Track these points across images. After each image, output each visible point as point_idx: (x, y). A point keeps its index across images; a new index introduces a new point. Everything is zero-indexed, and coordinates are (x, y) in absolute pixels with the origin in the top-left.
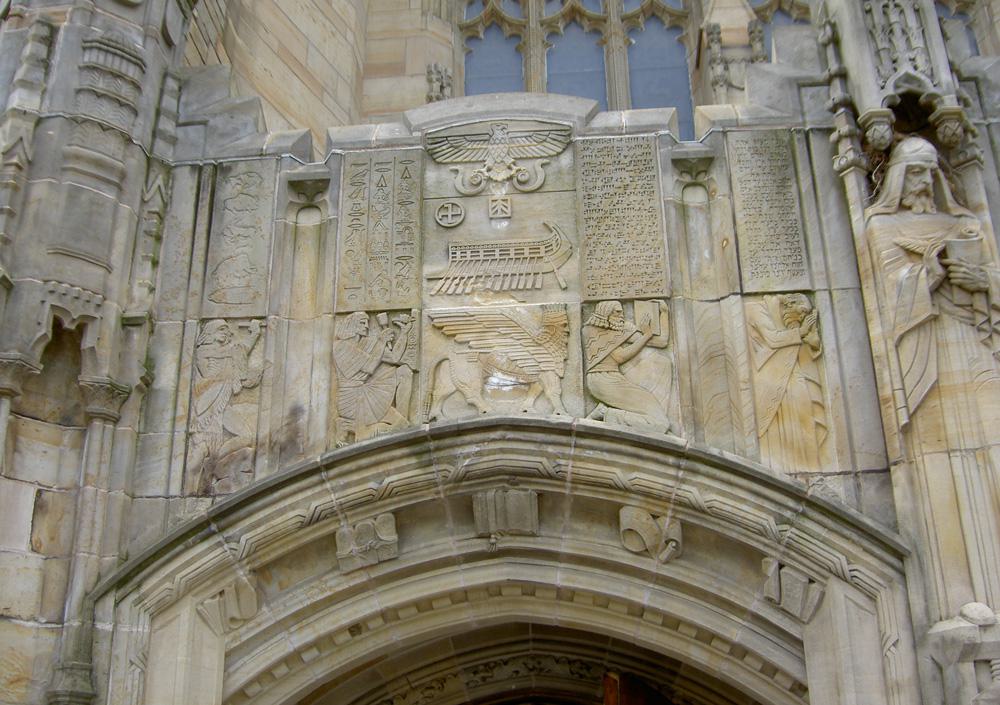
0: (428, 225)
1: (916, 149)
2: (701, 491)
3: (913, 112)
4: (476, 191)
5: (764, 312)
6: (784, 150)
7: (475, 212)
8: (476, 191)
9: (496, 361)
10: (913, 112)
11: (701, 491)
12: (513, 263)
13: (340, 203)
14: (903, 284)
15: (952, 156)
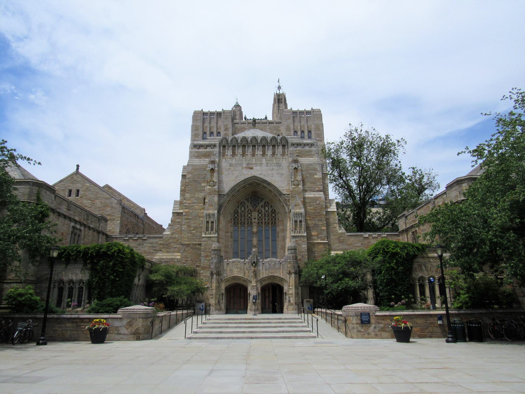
3: (254, 262)
9: (236, 273)
15: (256, 265)
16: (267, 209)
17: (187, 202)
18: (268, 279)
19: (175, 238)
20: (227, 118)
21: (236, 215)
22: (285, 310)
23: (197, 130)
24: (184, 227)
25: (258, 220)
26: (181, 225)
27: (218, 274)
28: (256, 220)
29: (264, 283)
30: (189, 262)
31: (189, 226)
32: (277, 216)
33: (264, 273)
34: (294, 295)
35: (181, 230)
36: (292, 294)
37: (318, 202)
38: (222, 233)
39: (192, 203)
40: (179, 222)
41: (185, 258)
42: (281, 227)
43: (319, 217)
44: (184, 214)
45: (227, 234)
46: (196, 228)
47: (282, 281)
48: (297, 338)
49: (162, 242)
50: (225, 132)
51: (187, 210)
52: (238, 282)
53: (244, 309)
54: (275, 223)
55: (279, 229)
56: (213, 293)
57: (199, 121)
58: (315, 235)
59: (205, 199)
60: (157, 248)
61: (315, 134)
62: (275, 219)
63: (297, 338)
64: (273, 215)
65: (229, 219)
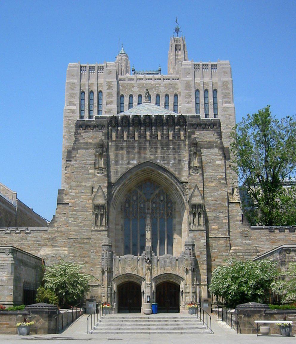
0: (125, 263)
1: (148, 261)
2: (137, 276)
3: (148, 259)
4: (128, 261)
5: (141, 268)
6: (143, 259)
7: (128, 262)
8: (128, 261)
9: (129, 270)
10: (148, 259)
11: (137, 276)
12: (129, 265)
13: (121, 261)
14: (147, 268)
16: (162, 198)
17: (74, 191)
18: (164, 277)
19: (61, 231)
20: (110, 73)
21: (127, 206)
22: (181, 310)
23: (73, 89)
24: (71, 220)
25: (152, 210)
26: (68, 217)
27: (110, 271)
28: (150, 211)
29: (160, 281)
30: (77, 258)
31: (76, 219)
32: (174, 206)
33: (157, 272)
34: (191, 293)
35: (68, 223)
36: (189, 293)
37: (219, 192)
38: (112, 226)
39: (78, 193)
40: (65, 214)
41: (72, 253)
42: (178, 219)
43: (220, 208)
44: (70, 204)
45: (117, 226)
46: (84, 220)
47: (178, 279)
48: (192, 333)
49: (47, 236)
50: (108, 91)
51: (74, 200)
52: (131, 280)
53: (137, 308)
54: (171, 214)
55: (176, 221)
56: (103, 291)
57: (75, 77)
58: (215, 229)
59: (93, 188)
60: (42, 243)
61: (223, 93)
62: (171, 210)
63: (192, 333)
64: (169, 205)
65: (120, 210)
